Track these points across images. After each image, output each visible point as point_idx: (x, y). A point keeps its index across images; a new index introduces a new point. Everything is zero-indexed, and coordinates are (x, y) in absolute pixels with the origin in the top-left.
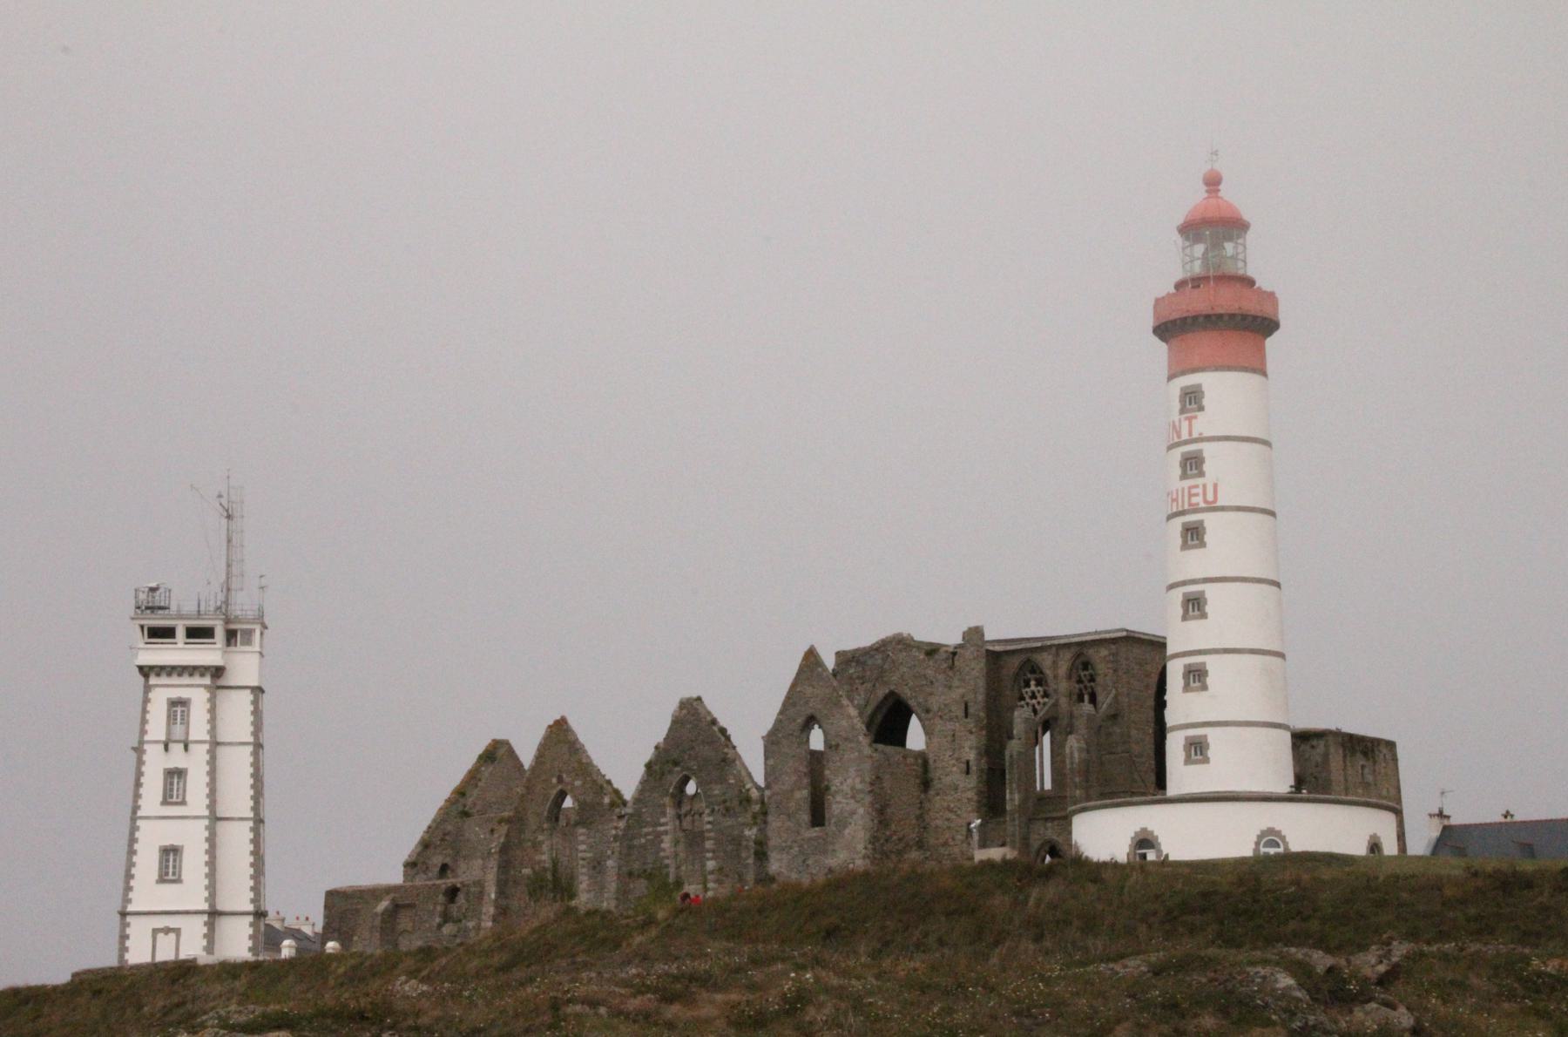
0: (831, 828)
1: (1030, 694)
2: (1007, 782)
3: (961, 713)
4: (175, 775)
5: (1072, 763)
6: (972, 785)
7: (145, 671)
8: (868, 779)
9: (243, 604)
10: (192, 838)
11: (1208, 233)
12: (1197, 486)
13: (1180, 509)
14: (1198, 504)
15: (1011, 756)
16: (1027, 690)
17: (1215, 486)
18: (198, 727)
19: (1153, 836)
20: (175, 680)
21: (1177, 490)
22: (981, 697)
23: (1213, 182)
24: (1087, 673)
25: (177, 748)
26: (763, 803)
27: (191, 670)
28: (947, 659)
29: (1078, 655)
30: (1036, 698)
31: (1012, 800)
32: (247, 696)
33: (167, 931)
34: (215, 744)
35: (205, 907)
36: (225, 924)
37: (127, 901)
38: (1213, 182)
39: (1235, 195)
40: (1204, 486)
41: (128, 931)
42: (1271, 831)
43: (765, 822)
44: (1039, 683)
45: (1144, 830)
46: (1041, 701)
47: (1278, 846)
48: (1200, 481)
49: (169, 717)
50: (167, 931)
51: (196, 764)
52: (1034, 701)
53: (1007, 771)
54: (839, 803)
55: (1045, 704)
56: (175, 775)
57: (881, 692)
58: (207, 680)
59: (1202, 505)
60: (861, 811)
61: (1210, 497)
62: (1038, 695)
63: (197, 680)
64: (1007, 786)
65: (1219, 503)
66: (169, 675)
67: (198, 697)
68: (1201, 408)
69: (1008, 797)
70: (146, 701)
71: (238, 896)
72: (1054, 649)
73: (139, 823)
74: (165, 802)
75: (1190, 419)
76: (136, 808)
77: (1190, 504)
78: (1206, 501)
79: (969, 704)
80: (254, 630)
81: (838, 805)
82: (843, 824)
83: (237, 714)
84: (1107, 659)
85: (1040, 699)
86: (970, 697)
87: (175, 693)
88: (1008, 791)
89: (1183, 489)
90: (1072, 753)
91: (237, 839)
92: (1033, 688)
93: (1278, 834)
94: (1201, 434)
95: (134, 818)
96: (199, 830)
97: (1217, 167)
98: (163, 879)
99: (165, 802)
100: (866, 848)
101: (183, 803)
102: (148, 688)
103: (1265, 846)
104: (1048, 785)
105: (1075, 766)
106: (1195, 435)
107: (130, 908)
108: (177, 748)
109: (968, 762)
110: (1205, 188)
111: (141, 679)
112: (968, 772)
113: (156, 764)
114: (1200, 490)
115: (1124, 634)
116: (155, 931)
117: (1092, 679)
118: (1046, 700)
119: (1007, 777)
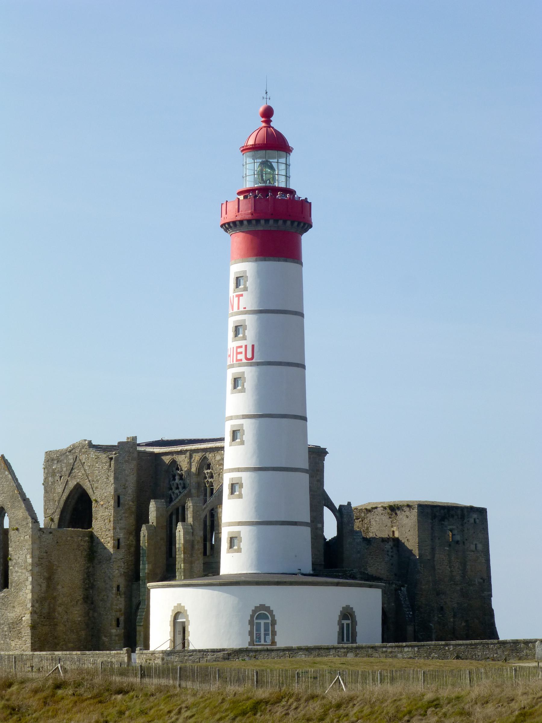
0: (12, 588)
1: (175, 486)
6: (121, 557)
12: (241, 347)
14: (241, 360)
17: (253, 346)
21: (233, 348)
23: (268, 114)
24: (209, 471)
28: (106, 462)
29: (204, 459)
30: (171, 489)
38: (268, 114)
40: (246, 346)
42: (263, 607)
47: (267, 618)
48: (243, 343)
54: (17, 572)
57: (72, 484)
60: (30, 579)
61: (249, 356)
62: (180, 486)
64: (141, 558)
69: (141, 567)
75: (239, 296)
77: (237, 360)
78: (247, 359)
79: (121, 496)
82: (19, 586)
85: (180, 489)
88: (141, 562)
90: (180, 536)
93: (268, 609)
94: (245, 308)
100: (32, 606)
106: (241, 309)
109: (119, 540)
114: (243, 350)
117: (212, 477)
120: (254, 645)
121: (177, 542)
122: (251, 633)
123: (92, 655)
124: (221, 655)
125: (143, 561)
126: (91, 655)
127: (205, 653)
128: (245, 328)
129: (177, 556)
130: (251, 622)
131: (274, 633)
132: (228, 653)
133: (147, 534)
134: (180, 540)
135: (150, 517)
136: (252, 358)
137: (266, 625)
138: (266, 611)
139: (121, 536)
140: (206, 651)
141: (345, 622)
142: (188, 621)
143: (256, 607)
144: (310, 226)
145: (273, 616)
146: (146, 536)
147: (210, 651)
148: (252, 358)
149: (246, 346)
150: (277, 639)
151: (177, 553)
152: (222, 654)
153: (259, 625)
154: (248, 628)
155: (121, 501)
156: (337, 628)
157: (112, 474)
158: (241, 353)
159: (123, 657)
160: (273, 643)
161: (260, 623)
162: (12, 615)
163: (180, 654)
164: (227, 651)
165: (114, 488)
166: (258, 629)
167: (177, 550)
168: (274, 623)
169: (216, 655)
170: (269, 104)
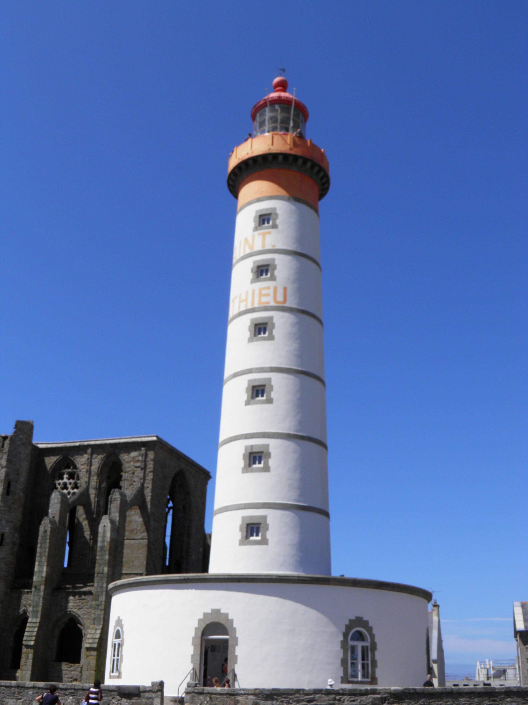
2: (38, 555)
5: (103, 542)
11: (294, 89)
12: (269, 288)
13: (249, 306)
14: (268, 303)
15: (45, 532)
16: (60, 481)
17: (285, 289)
19: (228, 620)
21: (247, 293)
22: (23, 479)
31: (40, 572)
42: (359, 621)
44: (71, 476)
45: (217, 612)
46: (72, 491)
48: (271, 284)
52: (65, 491)
53: (39, 545)
55: (74, 494)
59: (272, 304)
61: (280, 298)
62: (69, 486)
64: (37, 559)
69: (36, 569)
72: (89, 451)
75: (264, 235)
79: (12, 483)
84: (137, 459)
88: (37, 563)
89: (254, 291)
90: (104, 532)
92: (65, 480)
93: (365, 624)
94: (274, 246)
103: (353, 639)
104: (66, 565)
105: (106, 544)
114: (271, 292)
115: (155, 439)
118: (75, 490)
119: (38, 550)
120: (349, 682)
121: (100, 539)
122: (344, 662)
123: (72, 691)
124: (368, 701)
125: (40, 562)
126: (70, 691)
127: (337, 698)
128: (275, 267)
129: (98, 558)
130: (344, 644)
132: (382, 698)
133: (49, 529)
134: (104, 536)
135: (50, 511)
136: (285, 301)
138: (353, 628)
140: (341, 692)
142: (236, 640)
143: (351, 621)
145: (372, 636)
146: (49, 532)
147: (348, 692)
149: (275, 289)
151: (98, 553)
152: (371, 700)
153: (353, 649)
155: (12, 489)
157: (5, 457)
158: (268, 295)
159: (148, 698)
161: (357, 646)
163: (291, 697)
164: (379, 694)
165: (6, 472)
166: (354, 658)
167: (99, 549)
168: (374, 647)
169: (359, 701)
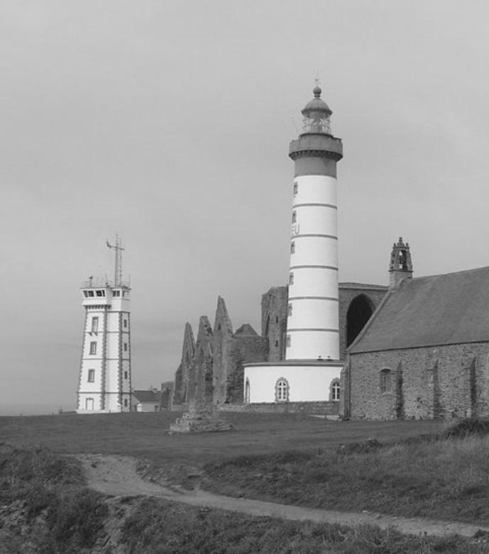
3: (275, 322)
4: (93, 344)
7: (87, 307)
8: (230, 350)
9: (124, 280)
10: (97, 366)
18: (101, 328)
20: (94, 310)
23: (318, 93)
25: (93, 334)
26: (212, 359)
27: (96, 306)
32: (117, 314)
33: (91, 399)
34: (106, 332)
35: (100, 391)
36: (128, 395)
37: (79, 388)
38: (318, 93)
39: (327, 99)
41: (80, 399)
43: (212, 366)
48: (294, 224)
49: (93, 323)
50: (91, 399)
51: (99, 339)
56: (93, 344)
58: (103, 310)
63: (100, 310)
65: (299, 234)
66: (93, 308)
67: (101, 316)
68: (297, 193)
70: (86, 318)
71: (114, 386)
73: (84, 361)
74: (91, 354)
76: (82, 356)
80: (118, 292)
81: (224, 361)
83: (114, 320)
86: (278, 314)
87: (96, 315)
91: (114, 367)
93: (285, 380)
95: (82, 359)
96: (99, 363)
97: (320, 87)
98: (89, 381)
99: (91, 354)
101: (95, 354)
102: (87, 313)
107: (80, 391)
108: (93, 334)
110: (314, 95)
111: (85, 310)
112: (277, 345)
113: (89, 339)
116: (87, 399)
122: (276, 394)
130: (276, 388)
131: (288, 394)
137: (284, 389)
139: (278, 339)
141: (336, 387)
144: (342, 157)
148: (298, 232)
150: (289, 398)
153: (280, 389)
154: (275, 391)
155: (279, 320)
156: (329, 391)
160: (288, 399)
162: (222, 383)
168: (288, 388)
170: (319, 86)
